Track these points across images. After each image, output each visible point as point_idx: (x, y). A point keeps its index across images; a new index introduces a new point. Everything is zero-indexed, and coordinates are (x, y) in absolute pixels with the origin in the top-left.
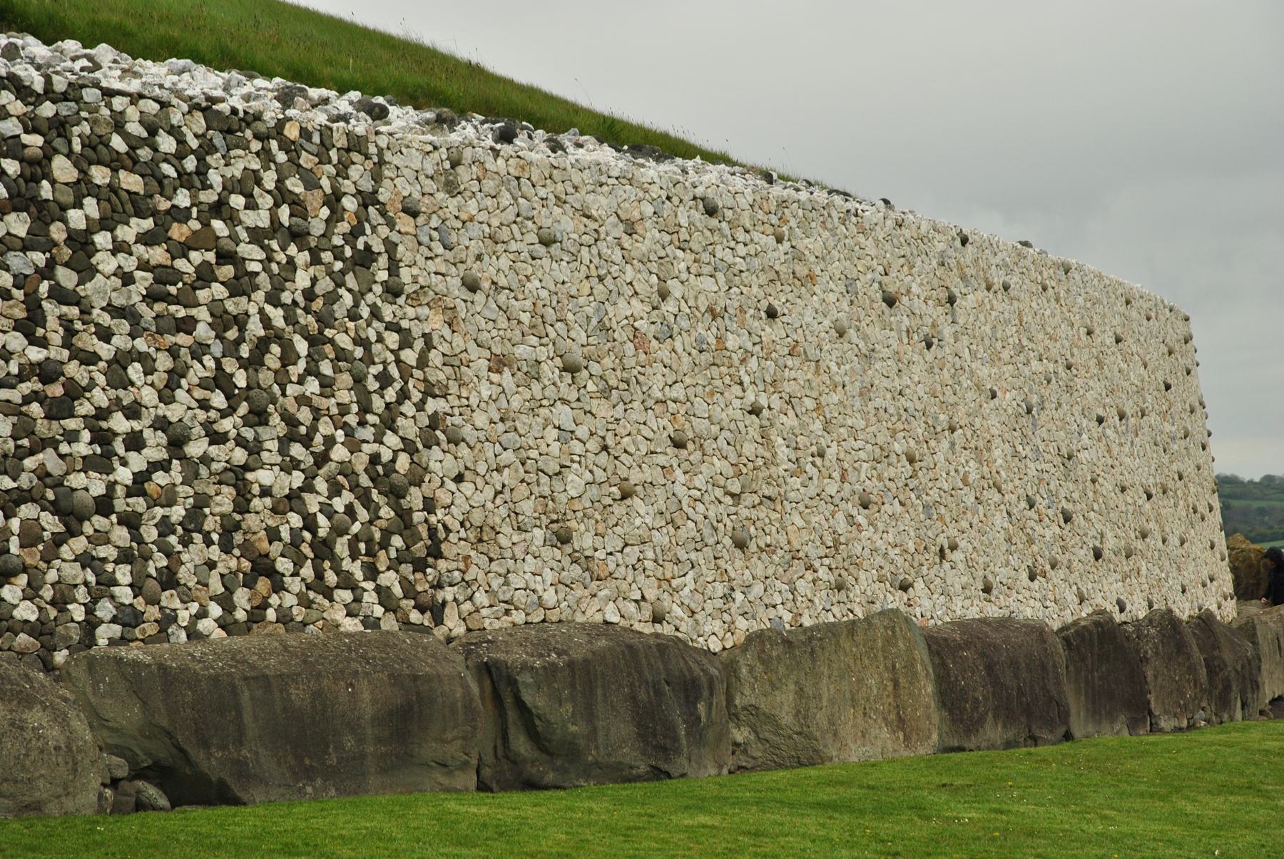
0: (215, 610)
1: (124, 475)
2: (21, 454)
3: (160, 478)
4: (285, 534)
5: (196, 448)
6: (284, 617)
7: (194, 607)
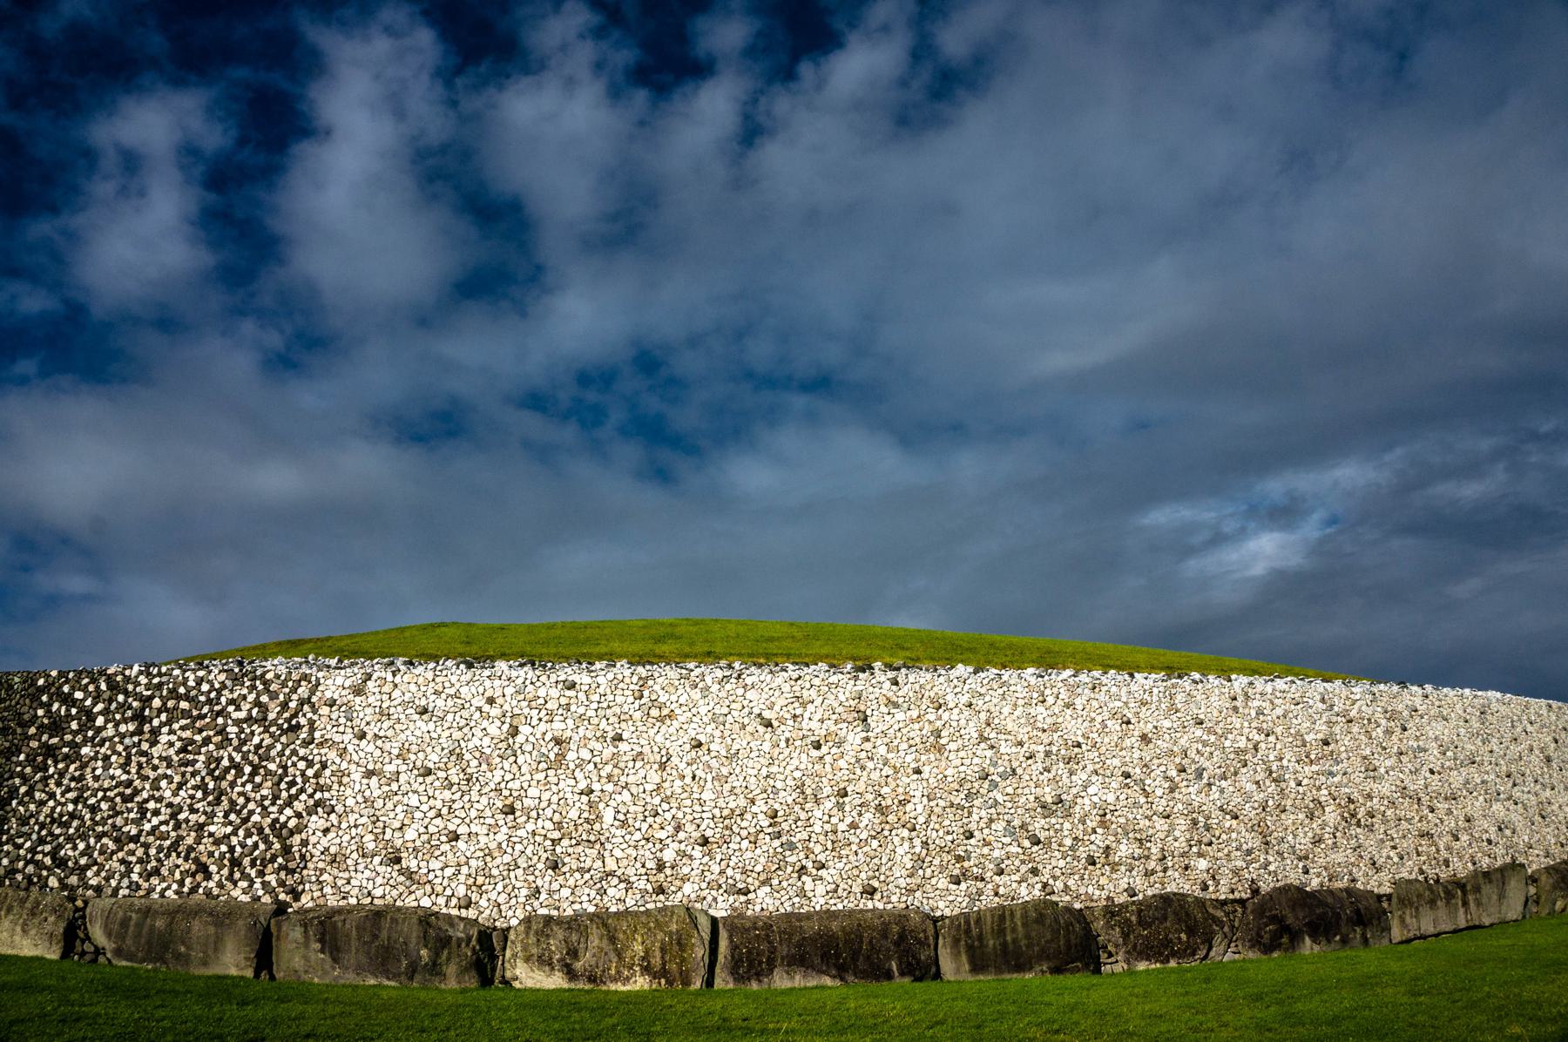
0: (175, 886)
1: (147, 827)
2: (110, 817)
3: (163, 828)
4: (217, 854)
5: (182, 816)
6: (208, 893)
7: (164, 885)
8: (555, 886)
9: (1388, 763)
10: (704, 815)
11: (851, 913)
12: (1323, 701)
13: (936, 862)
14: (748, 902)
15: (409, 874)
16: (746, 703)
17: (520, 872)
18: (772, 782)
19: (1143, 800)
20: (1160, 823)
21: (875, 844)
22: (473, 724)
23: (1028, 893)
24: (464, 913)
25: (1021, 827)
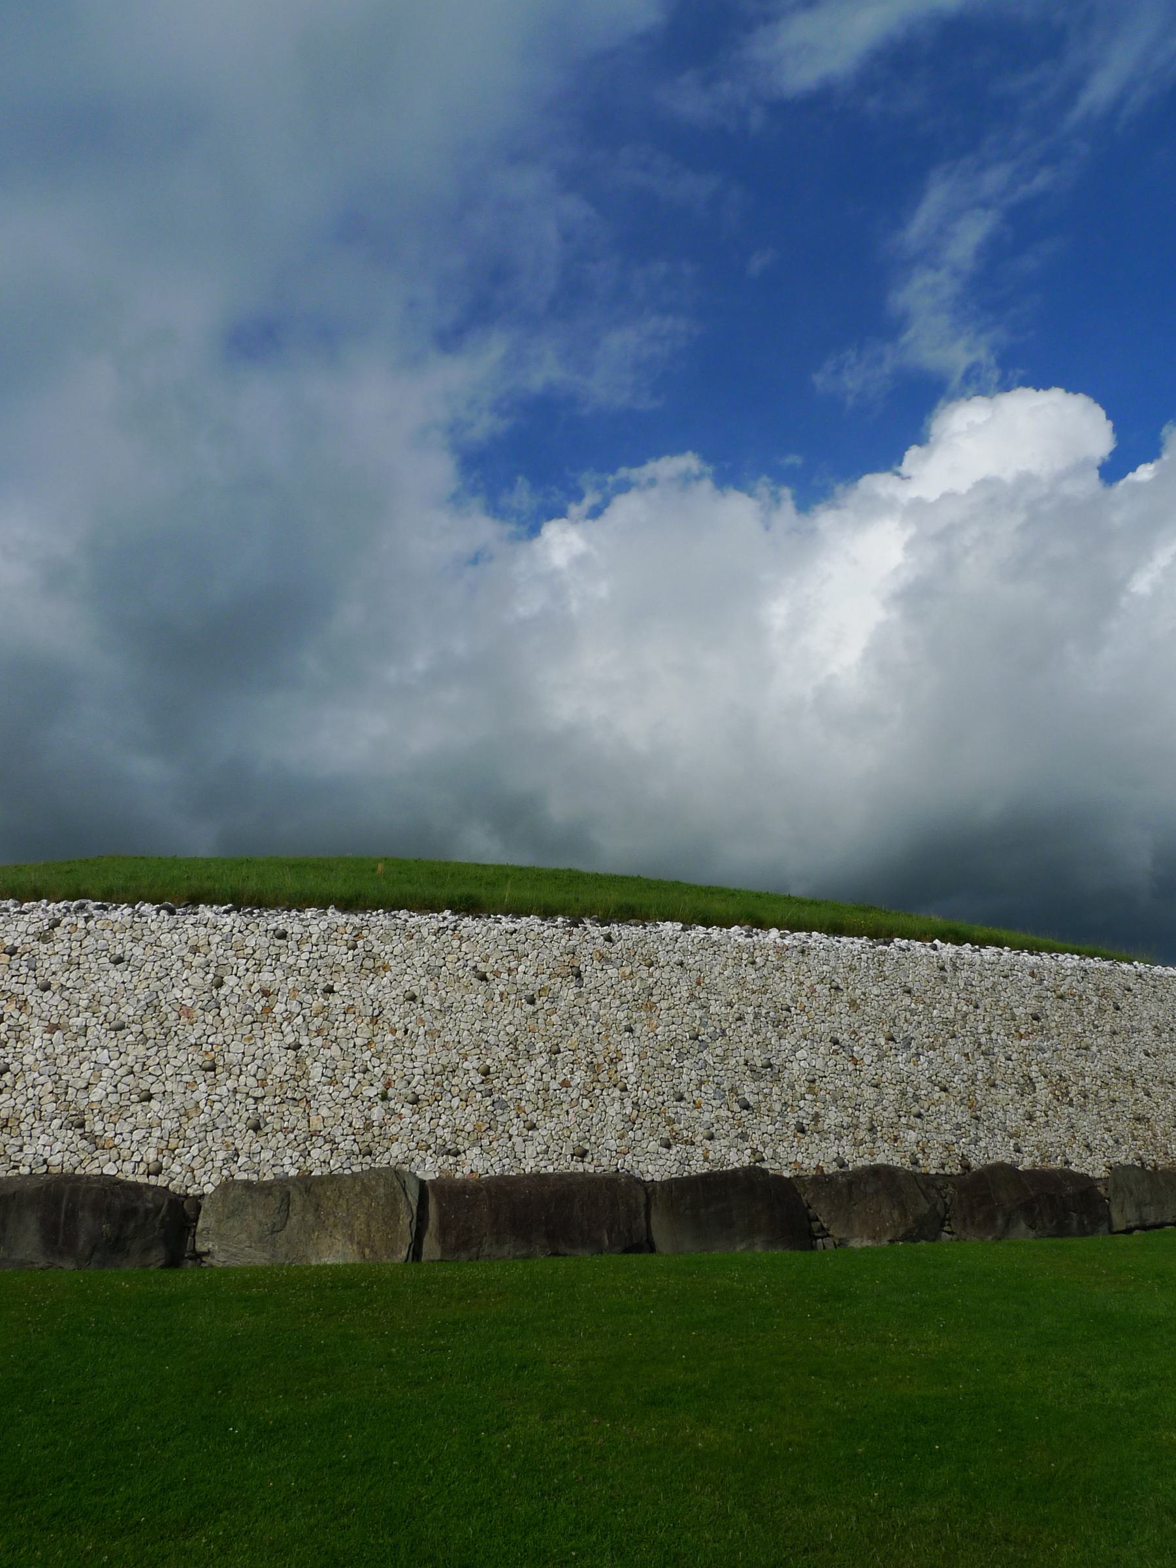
8: (256, 1147)
9: (1100, 1041)
10: (416, 1071)
11: (561, 1177)
12: (1032, 975)
13: (647, 1123)
14: (457, 1163)
15: (92, 1138)
16: (461, 955)
17: (219, 1132)
18: (485, 1037)
19: (851, 1067)
20: (869, 1093)
21: (586, 1103)
22: (173, 973)
23: (738, 1159)
24: (153, 1180)
25: (731, 1090)
